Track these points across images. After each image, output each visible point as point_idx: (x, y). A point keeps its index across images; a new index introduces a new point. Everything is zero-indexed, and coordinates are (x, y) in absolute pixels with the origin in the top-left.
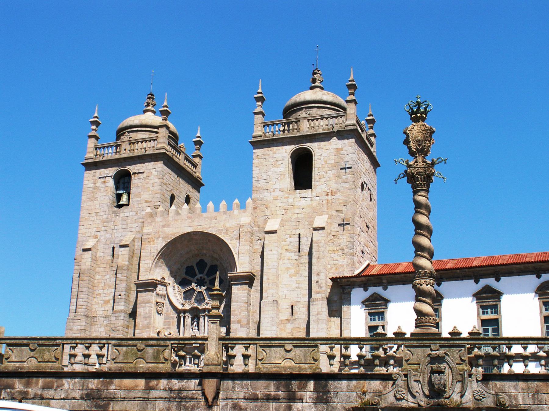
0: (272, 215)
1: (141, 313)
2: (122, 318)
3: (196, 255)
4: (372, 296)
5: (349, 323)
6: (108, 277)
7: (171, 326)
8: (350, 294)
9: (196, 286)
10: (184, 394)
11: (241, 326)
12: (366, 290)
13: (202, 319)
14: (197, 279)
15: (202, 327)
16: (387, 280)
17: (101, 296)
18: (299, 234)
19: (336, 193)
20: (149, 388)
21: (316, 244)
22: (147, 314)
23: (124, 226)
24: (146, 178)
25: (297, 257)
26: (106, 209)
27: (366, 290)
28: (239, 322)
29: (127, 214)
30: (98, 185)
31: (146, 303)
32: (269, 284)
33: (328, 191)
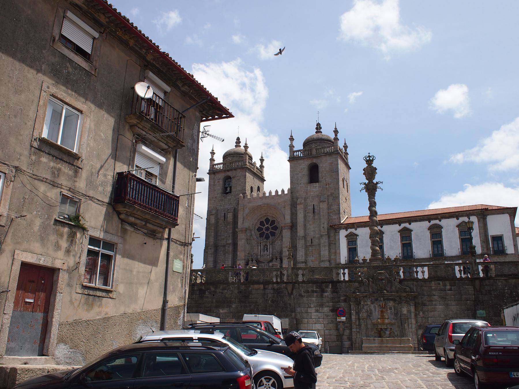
3: (265, 216)
4: (350, 233)
5: (339, 247)
6: (223, 227)
8: (339, 232)
9: (265, 231)
10: (280, 290)
12: (347, 231)
13: (269, 246)
16: (357, 225)
18: (314, 205)
19: (330, 184)
20: (264, 289)
23: (229, 203)
24: (238, 180)
25: (313, 216)
26: (220, 195)
27: (347, 231)
29: (230, 197)
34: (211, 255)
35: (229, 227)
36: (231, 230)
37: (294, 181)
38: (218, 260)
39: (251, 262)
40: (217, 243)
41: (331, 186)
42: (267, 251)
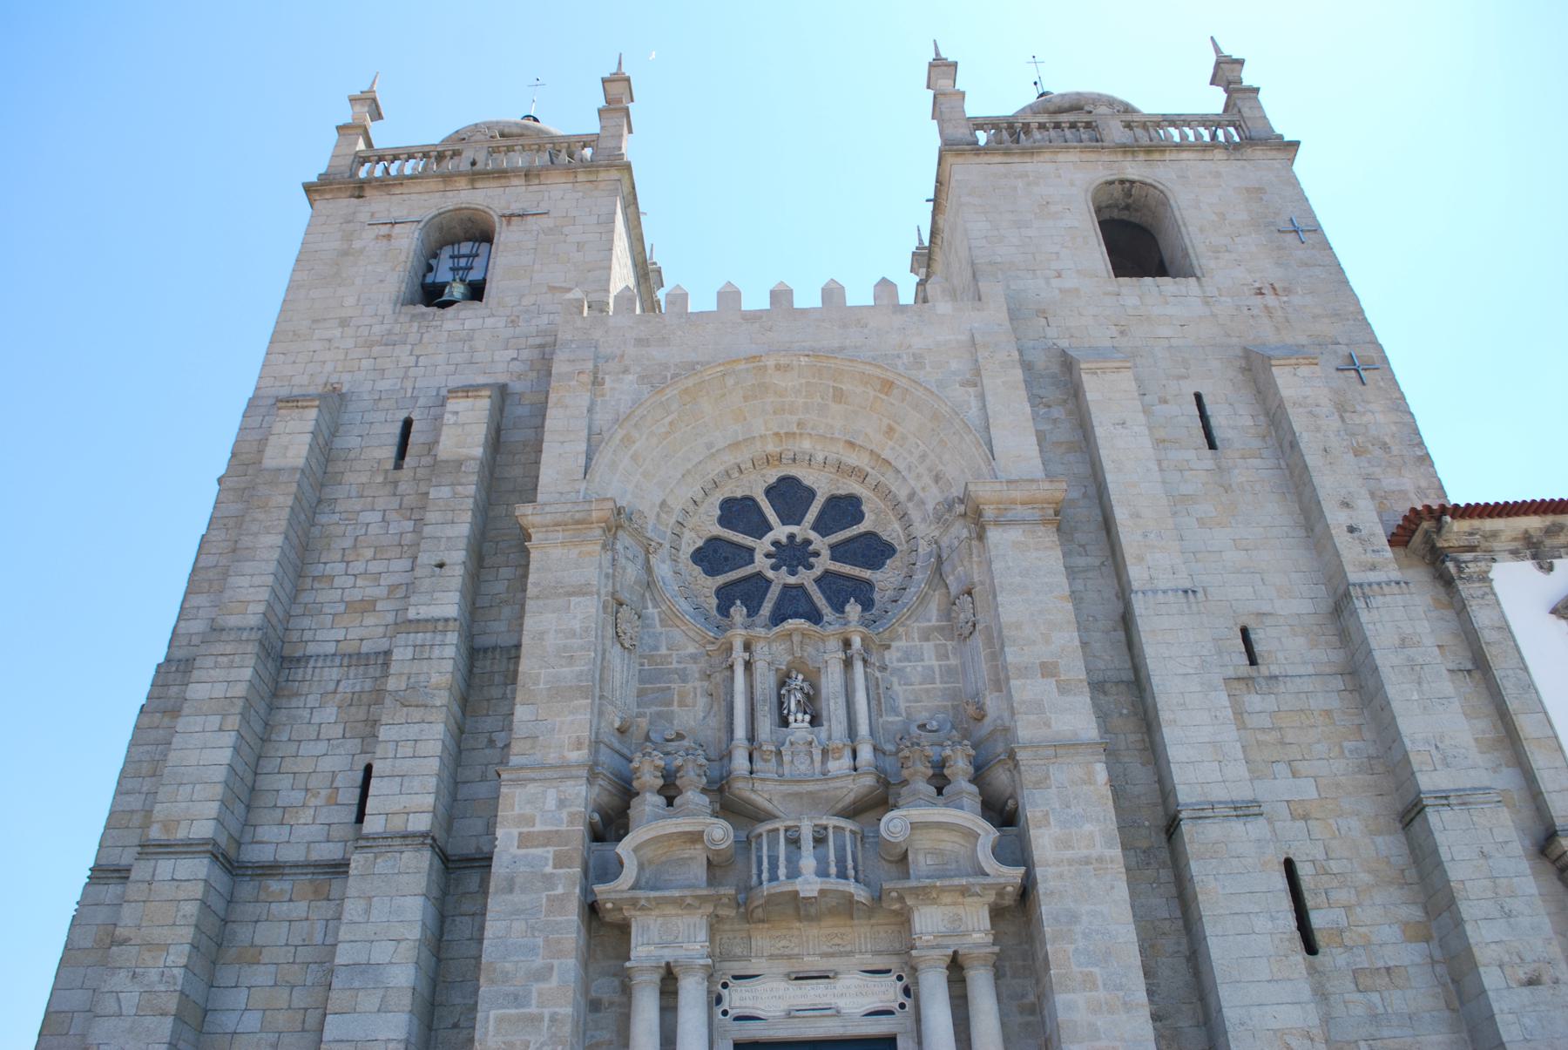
0: (1072, 336)
1: (541, 635)
2: (450, 652)
5: (1529, 686)
6: (377, 516)
7: (675, 708)
9: (775, 568)
11: (1063, 688)
13: (831, 682)
14: (776, 543)
15: (834, 709)
17: (337, 582)
18: (1198, 398)
19: (1288, 291)
21: (1301, 410)
22: (573, 634)
23: (458, 358)
26: (387, 308)
28: (1048, 670)
29: (468, 325)
30: (357, 245)
31: (570, 594)
32: (1145, 536)
33: (1257, 285)
34: (215, 721)
35: (445, 492)
36: (468, 517)
37: (999, 260)
38: (284, 782)
39: (660, 800)
40: (295, 636)
41: (1296, 300)
42: (816, 721)
